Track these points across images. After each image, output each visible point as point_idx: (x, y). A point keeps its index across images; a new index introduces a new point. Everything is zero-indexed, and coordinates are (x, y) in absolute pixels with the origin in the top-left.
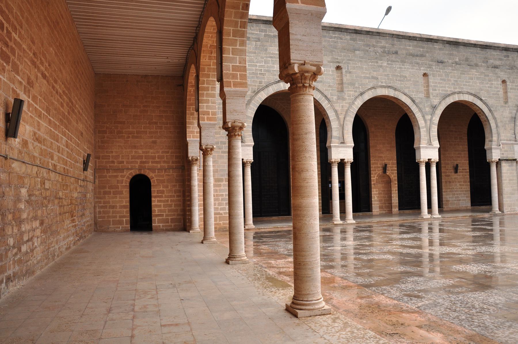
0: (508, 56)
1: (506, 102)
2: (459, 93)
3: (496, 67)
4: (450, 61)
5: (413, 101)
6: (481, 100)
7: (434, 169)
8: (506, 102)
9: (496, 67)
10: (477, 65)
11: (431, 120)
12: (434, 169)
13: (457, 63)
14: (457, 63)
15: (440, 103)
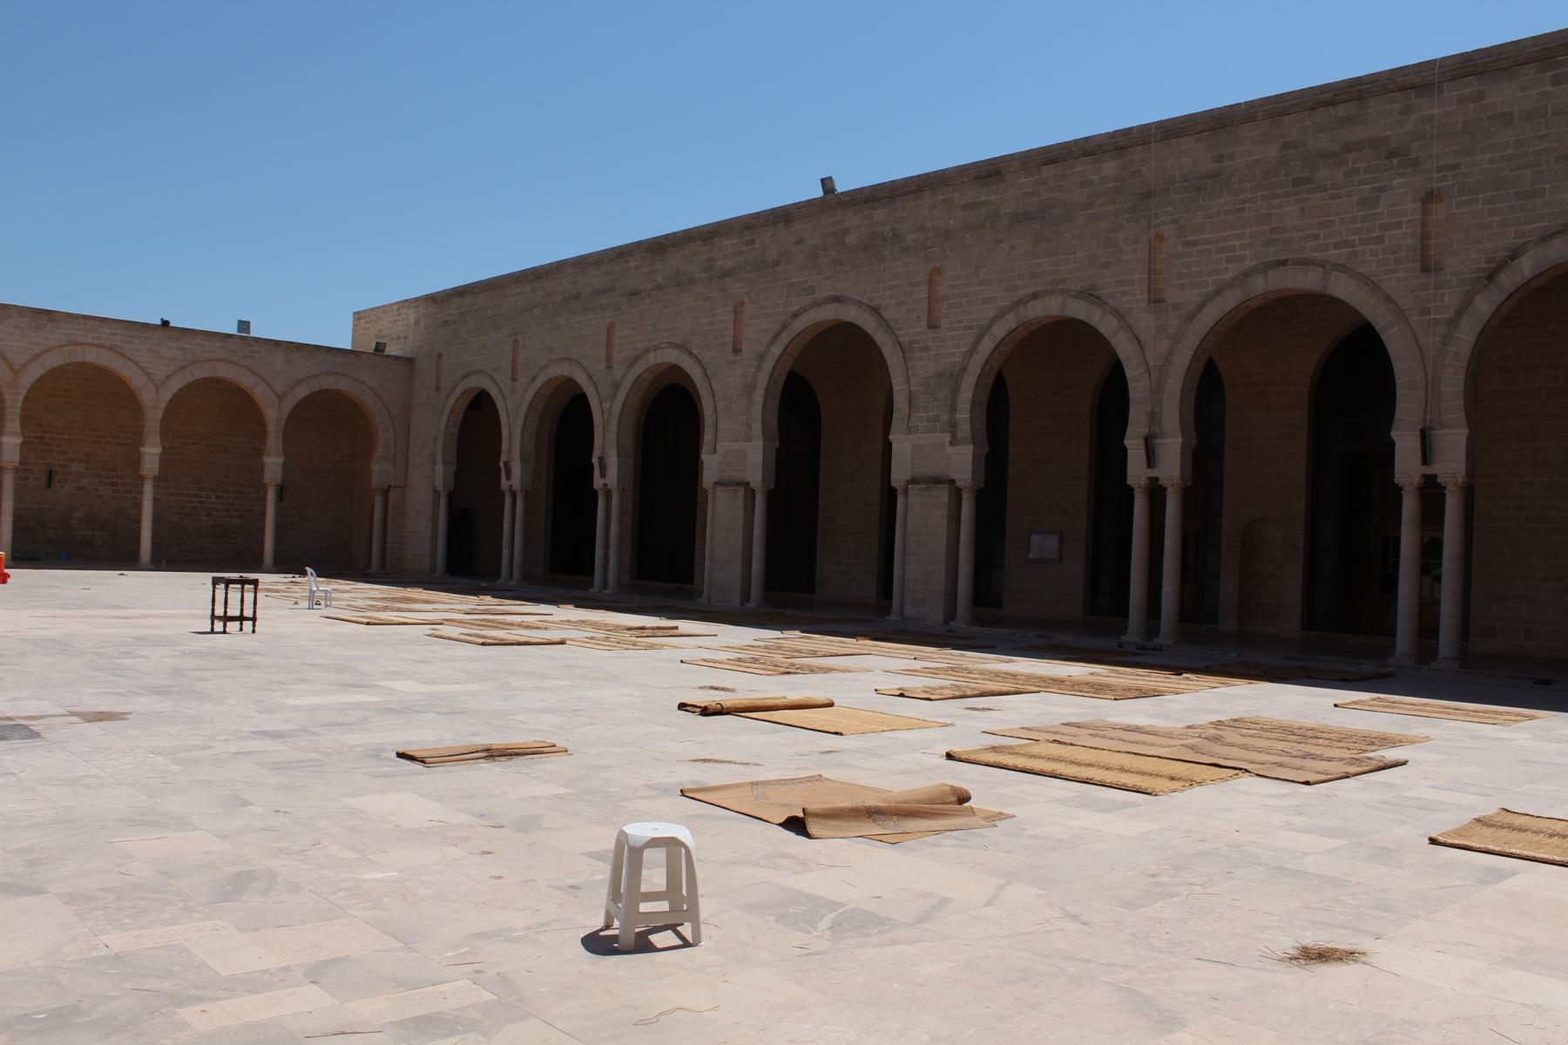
0: (753, 242)
1: (737, 350)
2: (657, 348)
3: (726, 274)
4: (649, 287)
5: (590, 377)
6: (690, 354)
7: (615, 502)
8: (737, 350)
9: (726, 274)
10: (692, 281)
11: (610, 411)
12: (615, 502)
13: (659, 288)
14: (659, 288)
15: (625, 374)
